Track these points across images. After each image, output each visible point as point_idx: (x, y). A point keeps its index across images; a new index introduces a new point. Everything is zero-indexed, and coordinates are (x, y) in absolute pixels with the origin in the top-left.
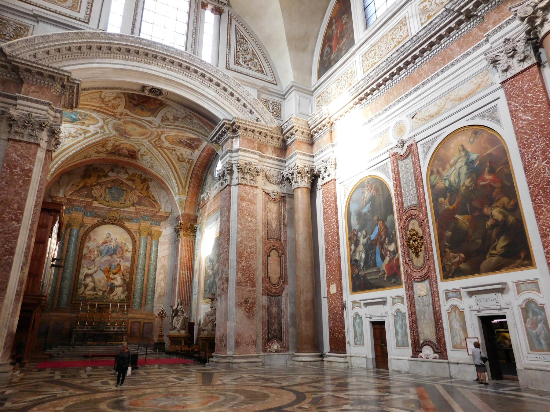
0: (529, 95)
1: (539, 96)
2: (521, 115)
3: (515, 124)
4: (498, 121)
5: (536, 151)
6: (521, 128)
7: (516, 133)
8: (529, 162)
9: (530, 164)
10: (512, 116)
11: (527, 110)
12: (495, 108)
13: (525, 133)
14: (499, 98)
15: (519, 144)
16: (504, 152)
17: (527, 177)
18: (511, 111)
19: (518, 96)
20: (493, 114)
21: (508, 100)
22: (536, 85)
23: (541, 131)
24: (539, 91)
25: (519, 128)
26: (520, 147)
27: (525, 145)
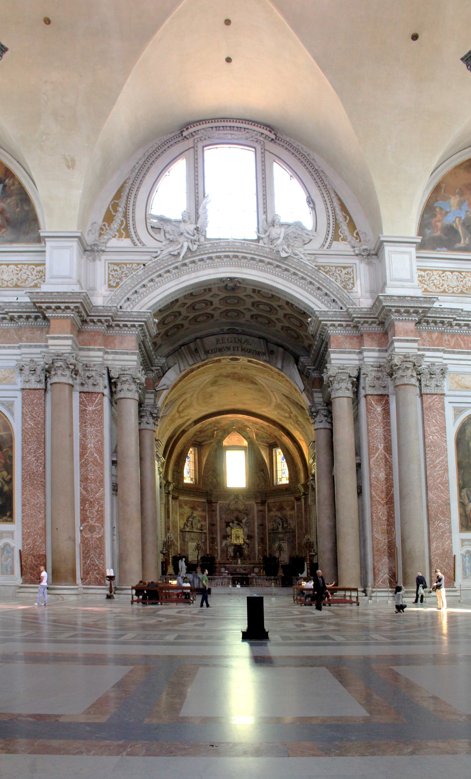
0: (36, 408)
1: (41, 412)
2: (28, 419)
3: (23, 425)
4: (12, 414)
5: (31, 449)
6: (27, 429)
7: (23, 430)
8: (26, 455)
9: (26, 457)
10: (22, 417)
11: (33, 418)
12: (12, 404)
13: (28, 434)
14: (16, 397)
15: (23, 439)
16: (11, 439)
17: (23, 464)
18: (23, 413)
19: (30, 405)
20: (10, 406)
21: (23, 404)
22: (41, 404)
23: (36, 437)
24: (41, 409)
25: (25, 428)
26: (23, 441)
27: (26, 441)
